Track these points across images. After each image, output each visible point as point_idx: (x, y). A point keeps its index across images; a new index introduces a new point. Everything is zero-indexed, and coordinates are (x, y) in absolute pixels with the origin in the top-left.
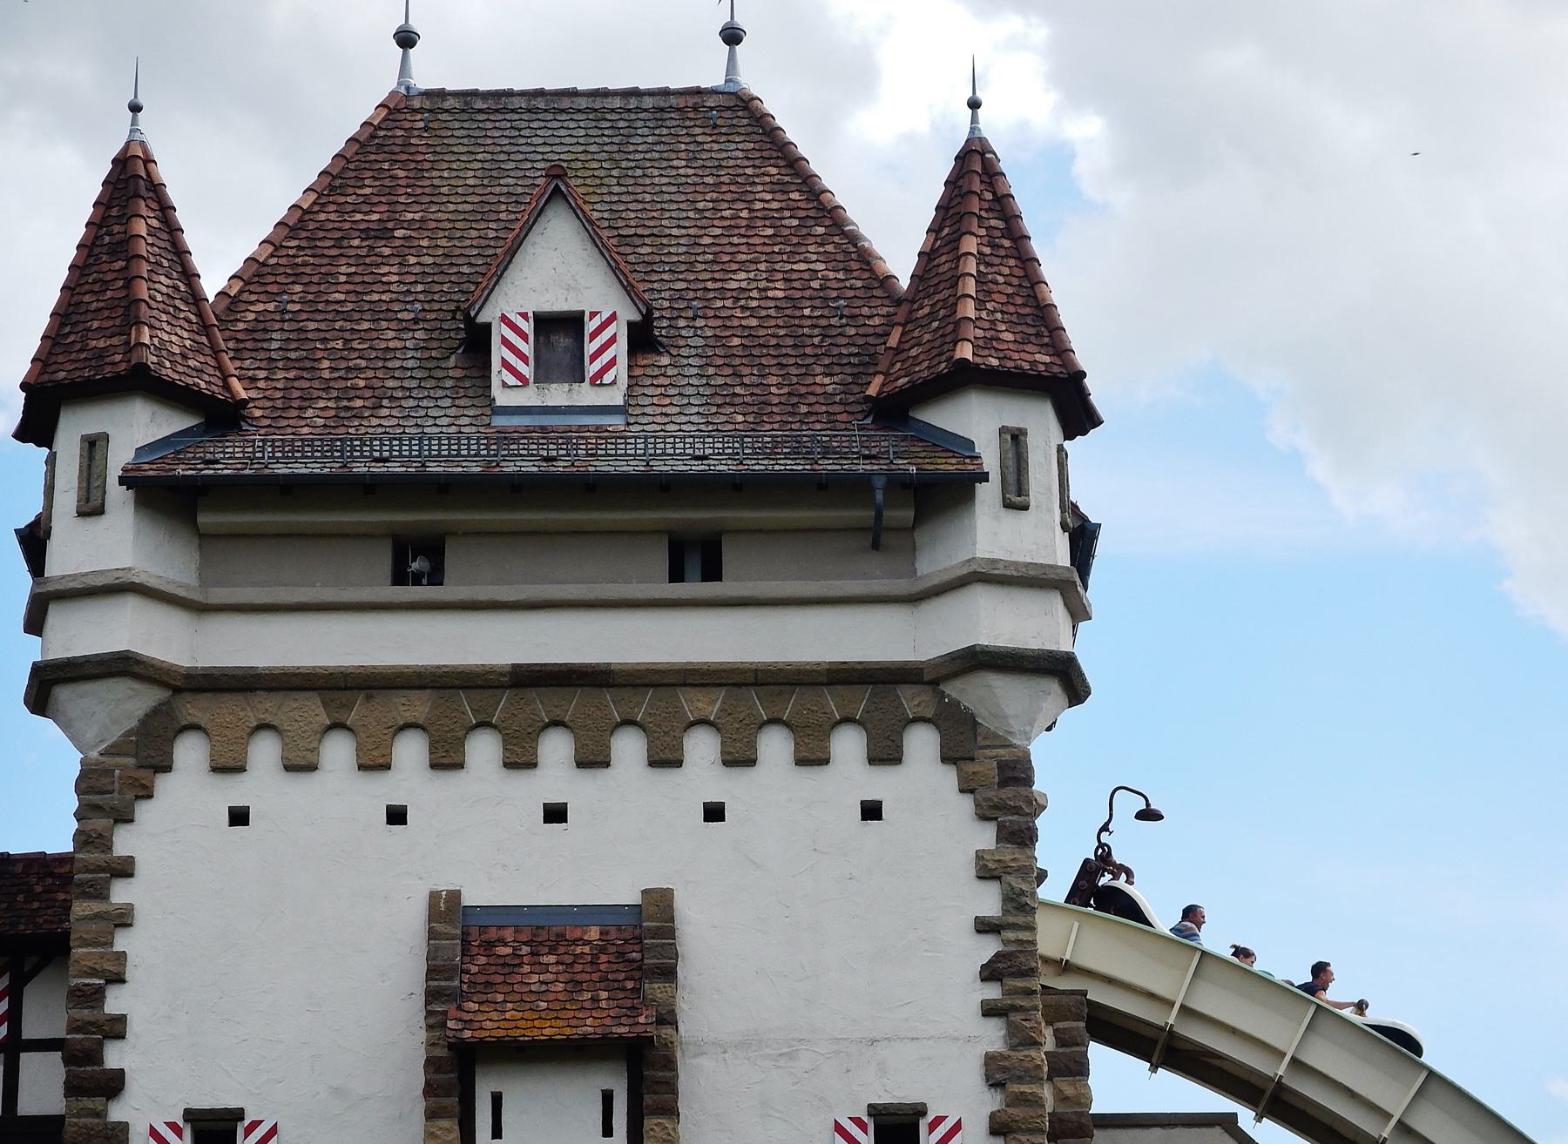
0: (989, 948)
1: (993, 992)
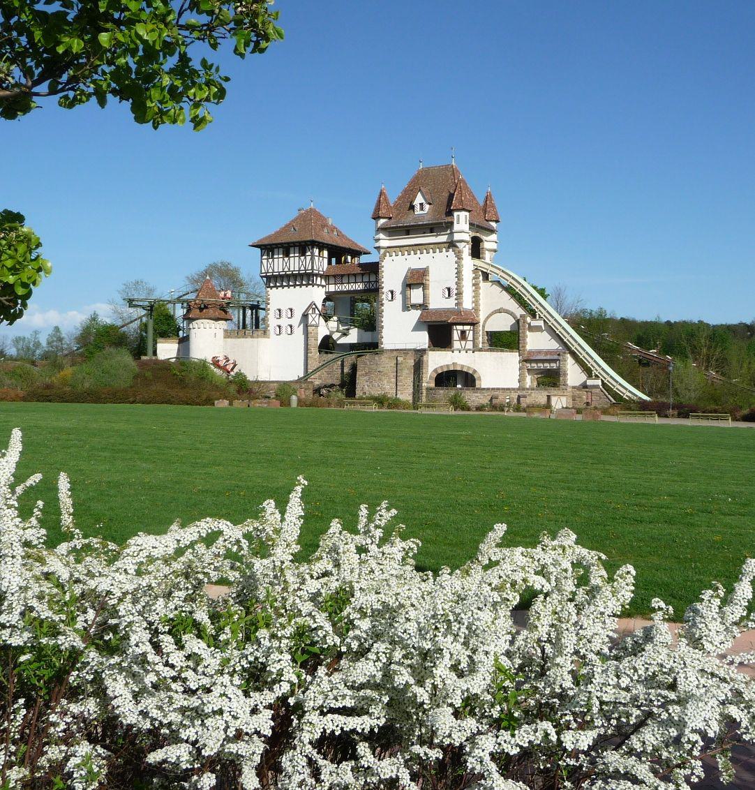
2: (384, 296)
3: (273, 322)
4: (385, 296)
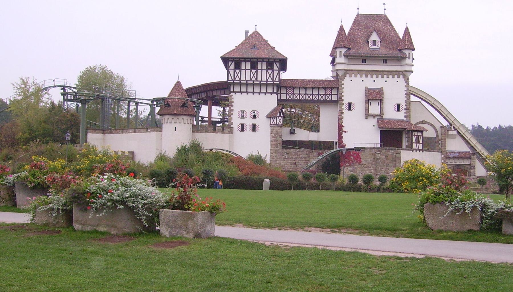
0: (406, 92)
1: (406, 96)
2: (344, 107)
3: (236, 121)
4: (345, 107)
